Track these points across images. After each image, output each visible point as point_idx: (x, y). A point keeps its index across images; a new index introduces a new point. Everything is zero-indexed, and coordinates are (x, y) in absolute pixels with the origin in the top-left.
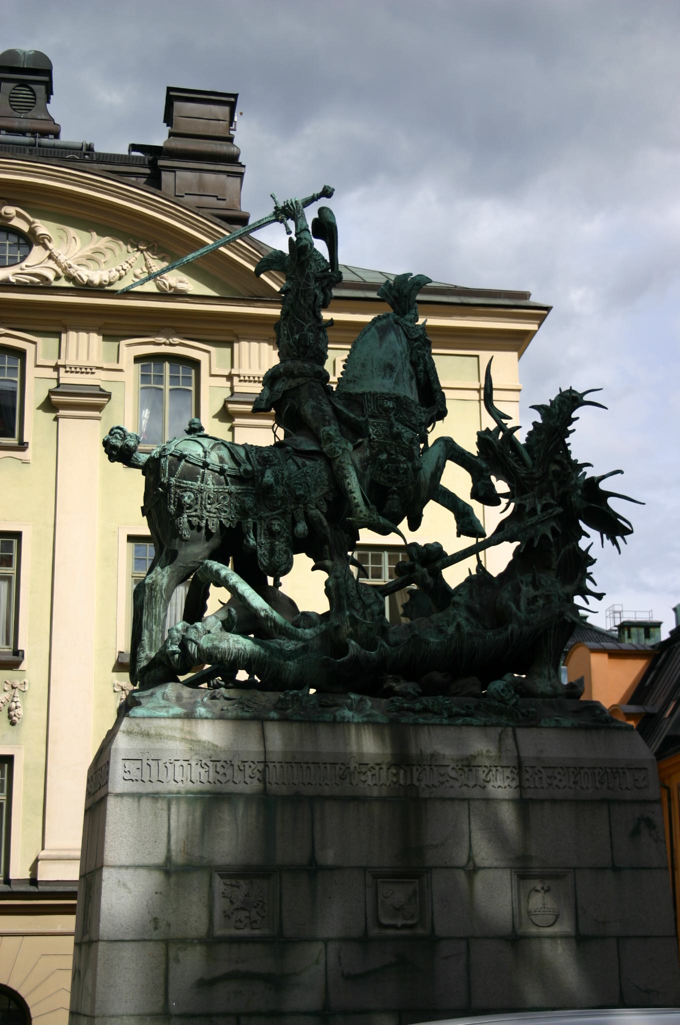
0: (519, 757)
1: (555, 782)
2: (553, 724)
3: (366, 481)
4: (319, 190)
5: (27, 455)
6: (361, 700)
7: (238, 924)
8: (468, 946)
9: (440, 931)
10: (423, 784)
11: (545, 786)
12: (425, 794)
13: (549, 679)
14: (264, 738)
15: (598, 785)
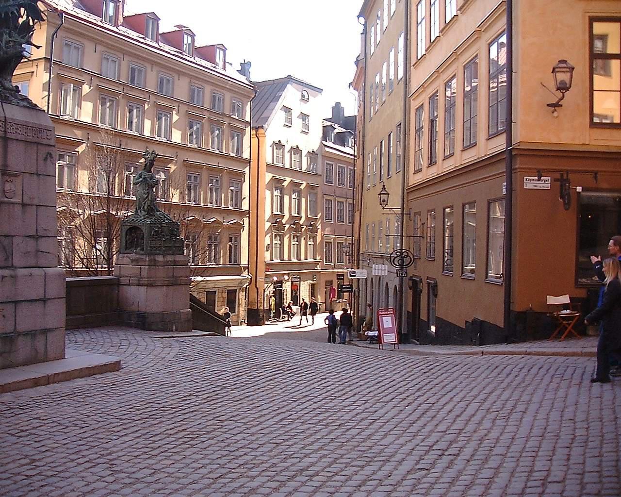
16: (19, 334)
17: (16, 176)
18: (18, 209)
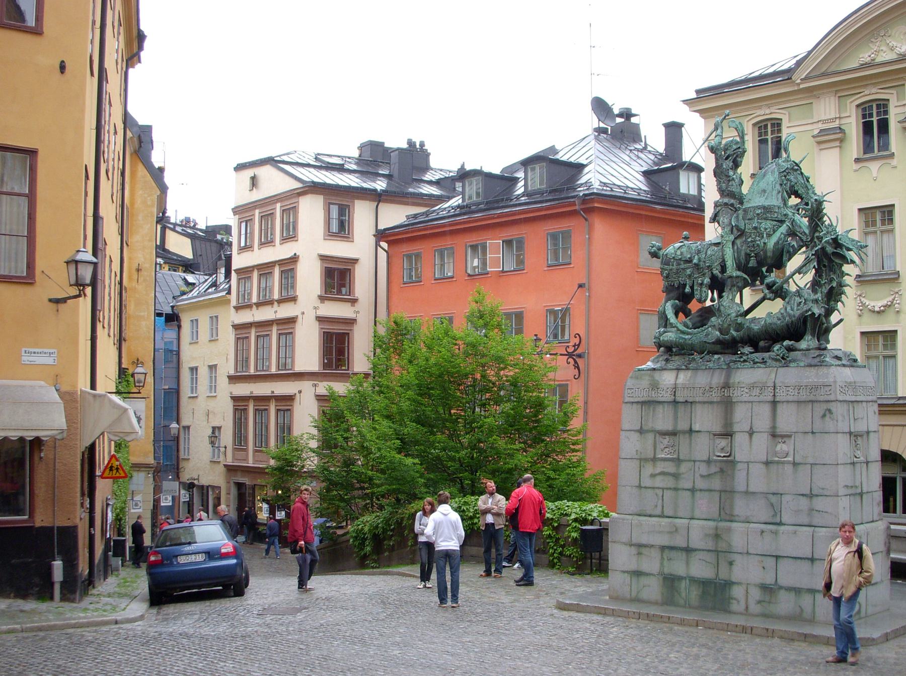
3: (743, 253)
16: (781, 588)
17: (789, 436)
18: (789, 469)
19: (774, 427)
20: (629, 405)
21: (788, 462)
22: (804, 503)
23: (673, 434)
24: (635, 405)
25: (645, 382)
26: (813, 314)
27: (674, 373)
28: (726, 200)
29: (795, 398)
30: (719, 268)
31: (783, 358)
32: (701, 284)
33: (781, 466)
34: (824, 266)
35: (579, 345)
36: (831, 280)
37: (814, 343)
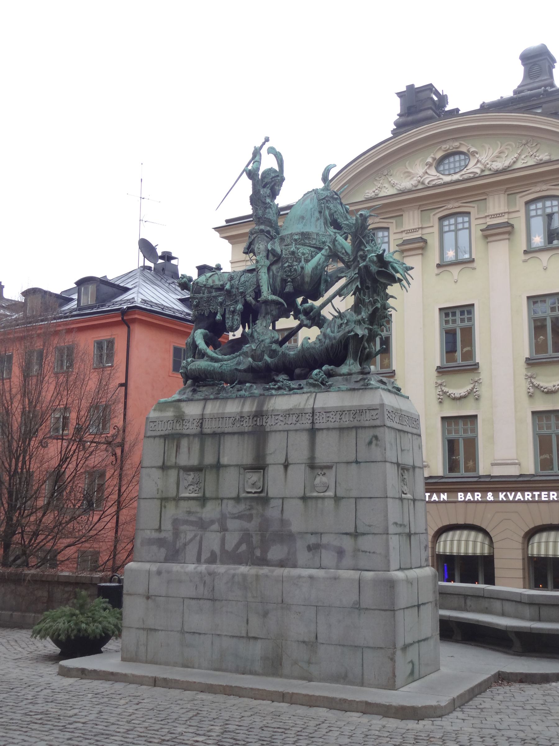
0: (313, 408)
1: (330, 419)
2: (337, 389)
3: (279, 279)
4: (264, 140)
5: (474, 265)
6: (251, 386)
7: (190, 492)
8: (283, 503)
9: (270, 495)
10: (268, 425)
11: (325, 422)
12: (268, 429)
13: (349, 365)
14: (204, 408)
15: (352, 419)
17: (329, 467)
18: (329, 504)
19: (312, 458)
20: (152, 440)
21: (330, 497)
22: (347, 543)
23: (199, 469)
24: (157, 440)
25: (170, 413)
26: (356, 335)
27: (201, 404)
28: (262, 227)
29: (337, 425)
30: (253, 294)
31: (322, 383)
32: (233, 312)
33: (320, 501)
34: (368, 288)
35: (117, 436)
36: (376, 301)
37: (356, 368)
